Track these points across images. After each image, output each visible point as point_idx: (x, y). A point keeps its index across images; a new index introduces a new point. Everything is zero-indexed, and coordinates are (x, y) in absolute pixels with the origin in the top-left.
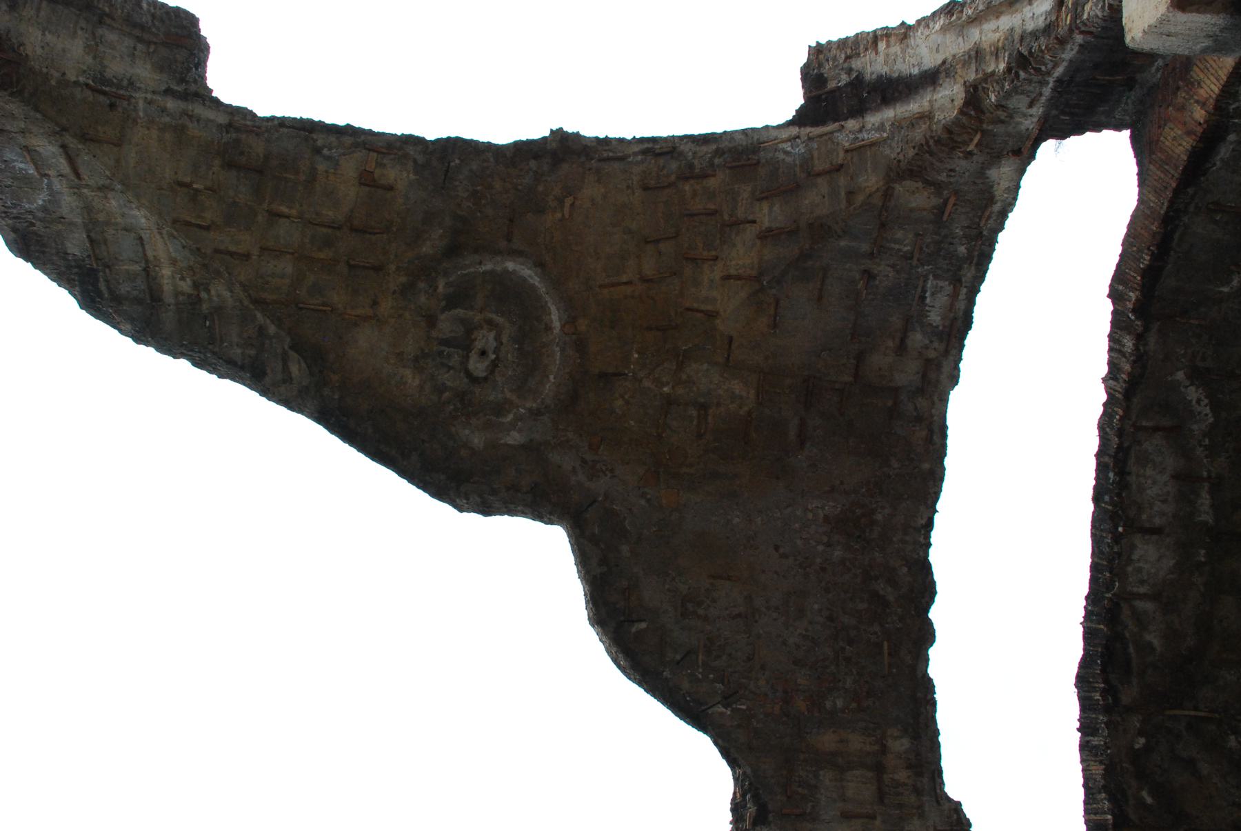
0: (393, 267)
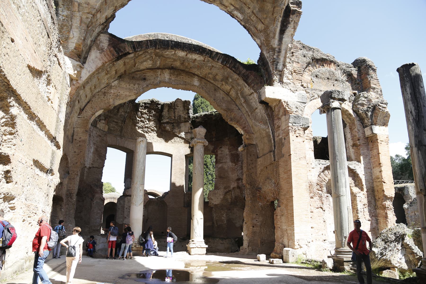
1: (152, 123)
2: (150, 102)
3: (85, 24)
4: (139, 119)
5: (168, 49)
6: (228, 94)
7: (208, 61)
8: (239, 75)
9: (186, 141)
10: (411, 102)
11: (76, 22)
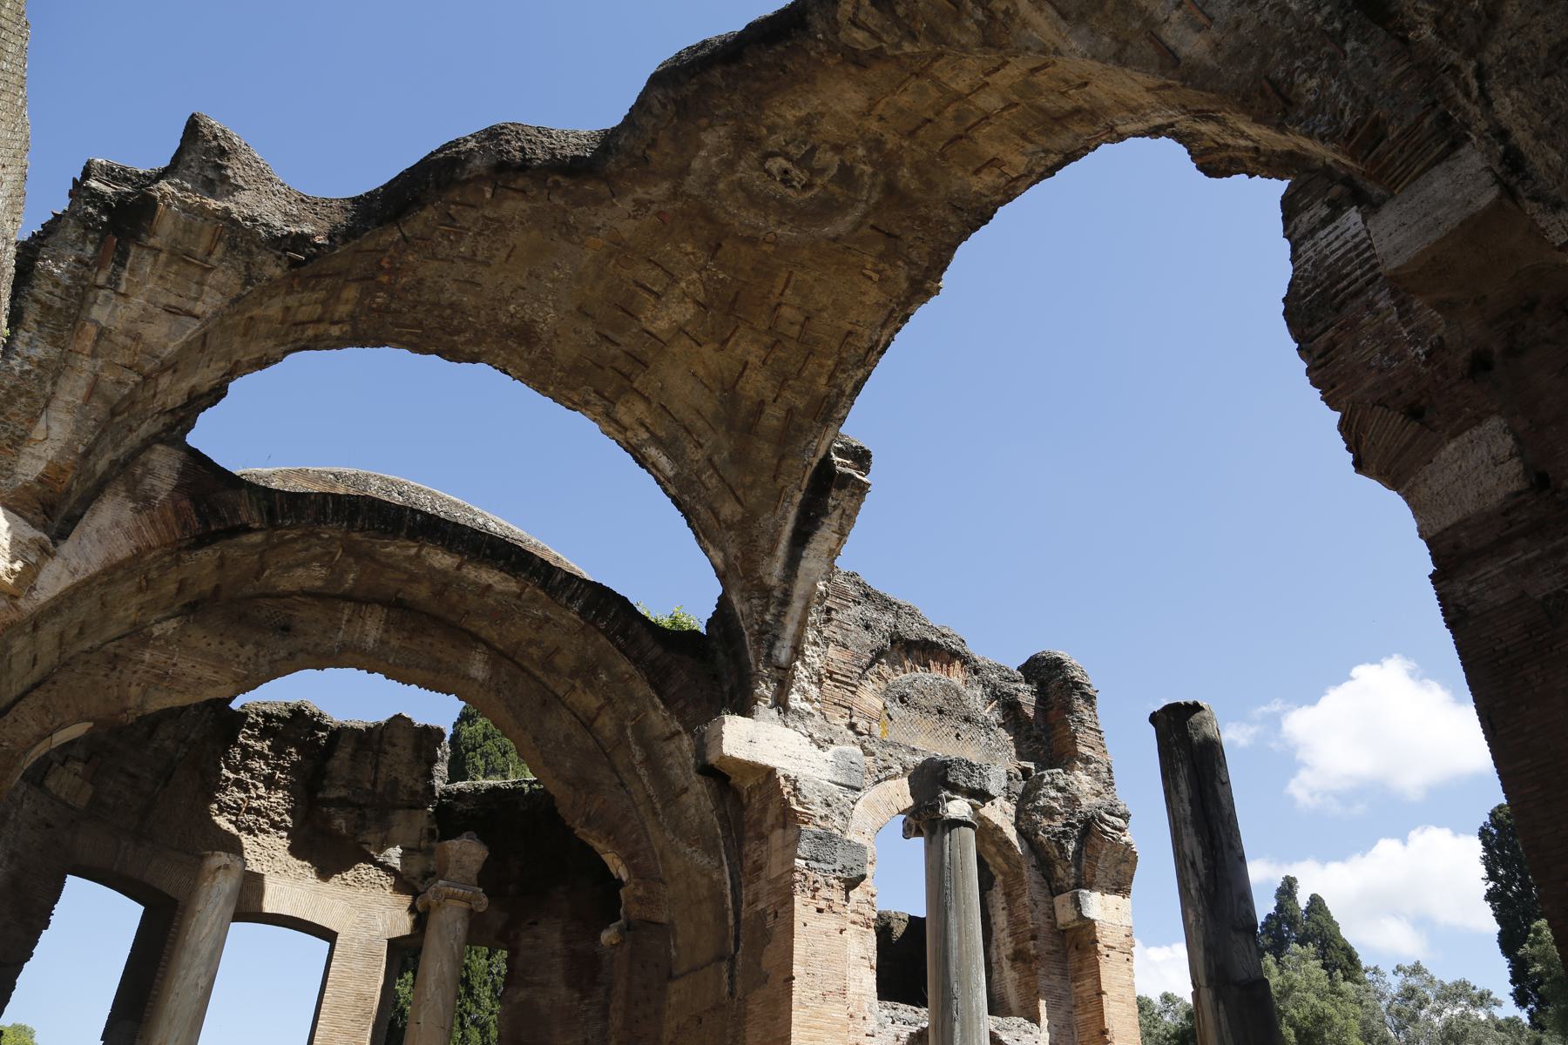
0: (905, 144)
1: (278, 796)
2: (287, 715)
3: (107, 400)
4: (231, 776)
5: (396, 537)
6: (587, 724)
7: (534, 599)
8: (636, 662)
9: (403, 883)
10: (1191, 830)
11: (72, 390)
